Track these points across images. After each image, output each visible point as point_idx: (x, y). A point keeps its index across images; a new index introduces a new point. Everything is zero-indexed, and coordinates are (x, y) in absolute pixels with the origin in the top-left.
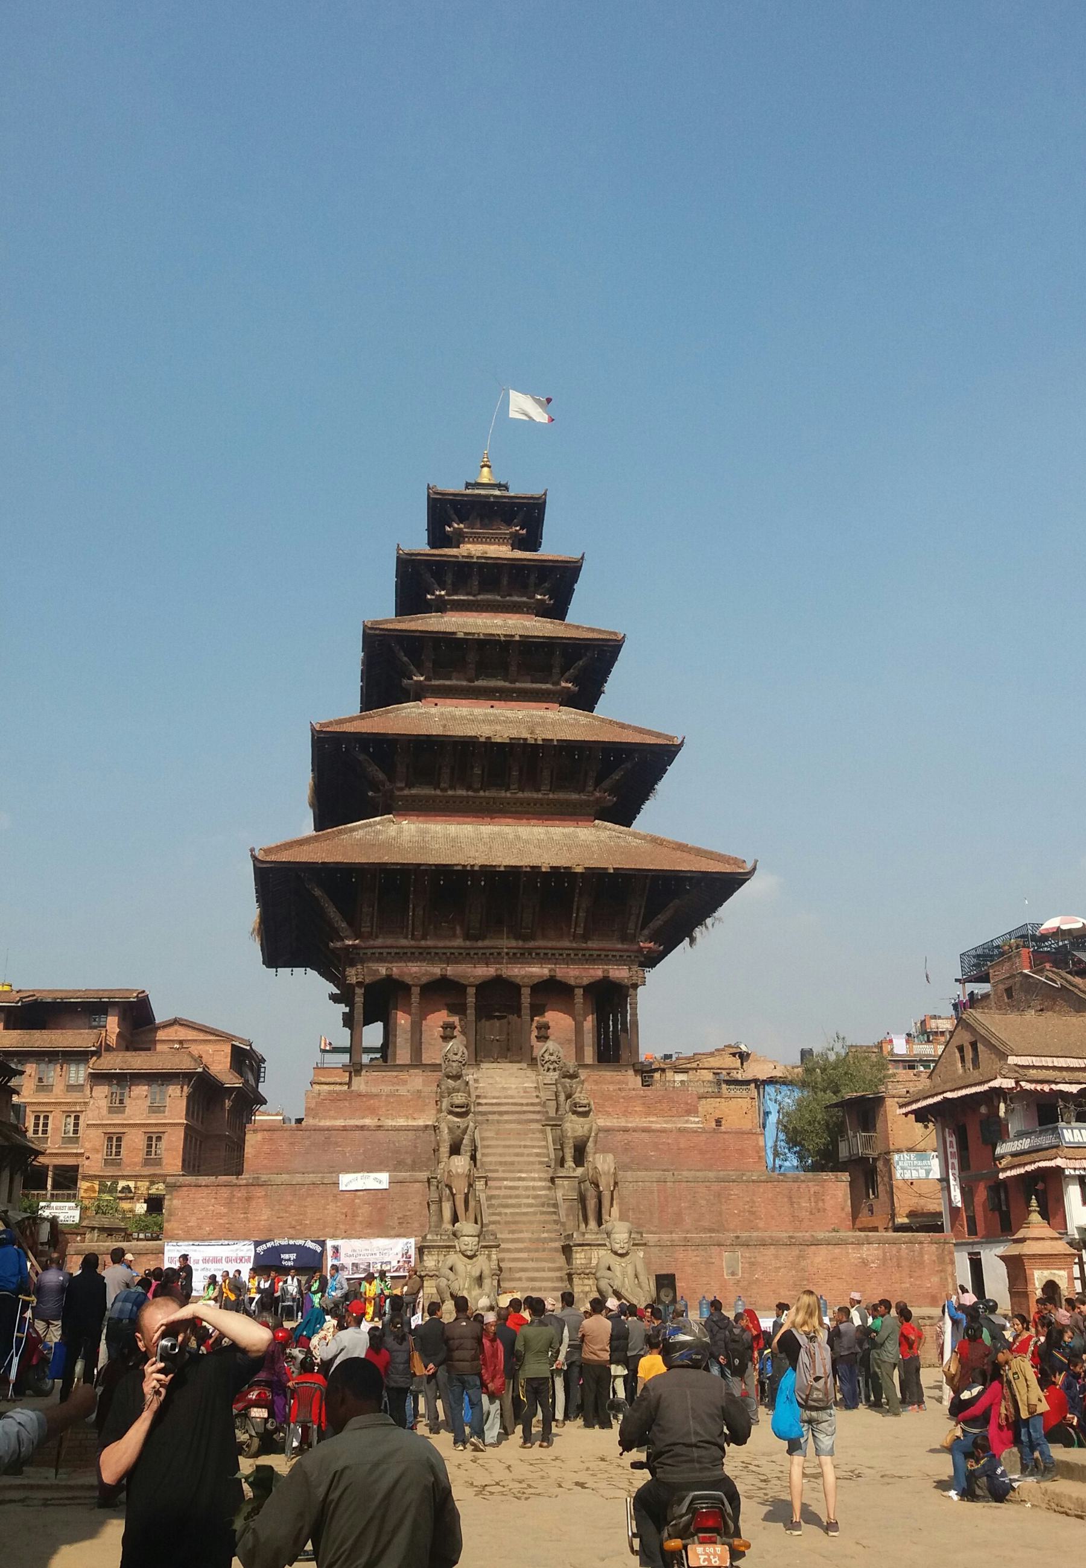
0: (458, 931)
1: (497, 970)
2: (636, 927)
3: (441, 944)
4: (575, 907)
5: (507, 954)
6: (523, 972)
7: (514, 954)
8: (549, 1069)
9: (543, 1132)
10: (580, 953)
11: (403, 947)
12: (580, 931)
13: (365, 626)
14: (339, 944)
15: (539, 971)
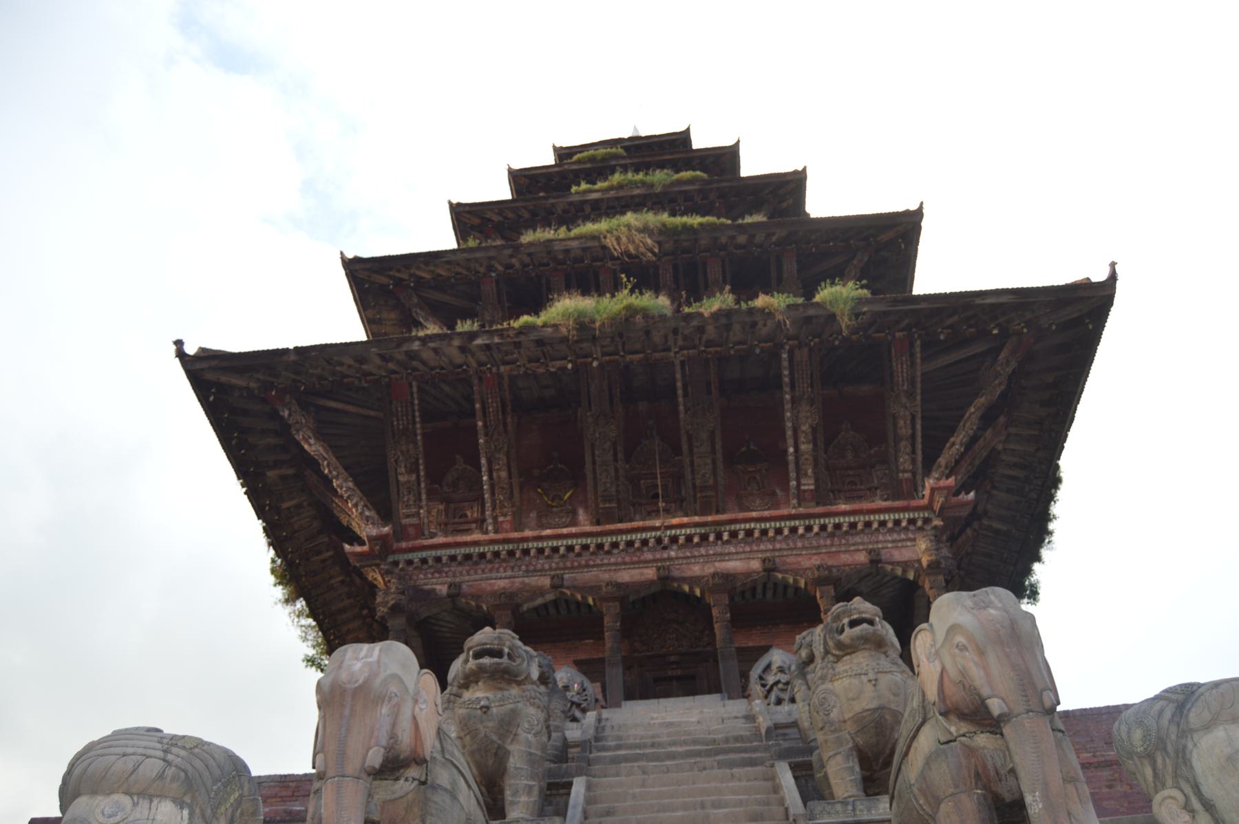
0: (582, 515)
1: (658, 569)
2: (914, 461)
3: (548, 532)
4: (789, 433)
5: (674, 540)
6: (712, 570)
7: (689, 538)
8: (779, 702)
9: (772, 778)
10: (816, 525)
11: (476, 543)
12: (808, 485)
13: (451, 204)
14: (358, 549)
15: (741, 563)
